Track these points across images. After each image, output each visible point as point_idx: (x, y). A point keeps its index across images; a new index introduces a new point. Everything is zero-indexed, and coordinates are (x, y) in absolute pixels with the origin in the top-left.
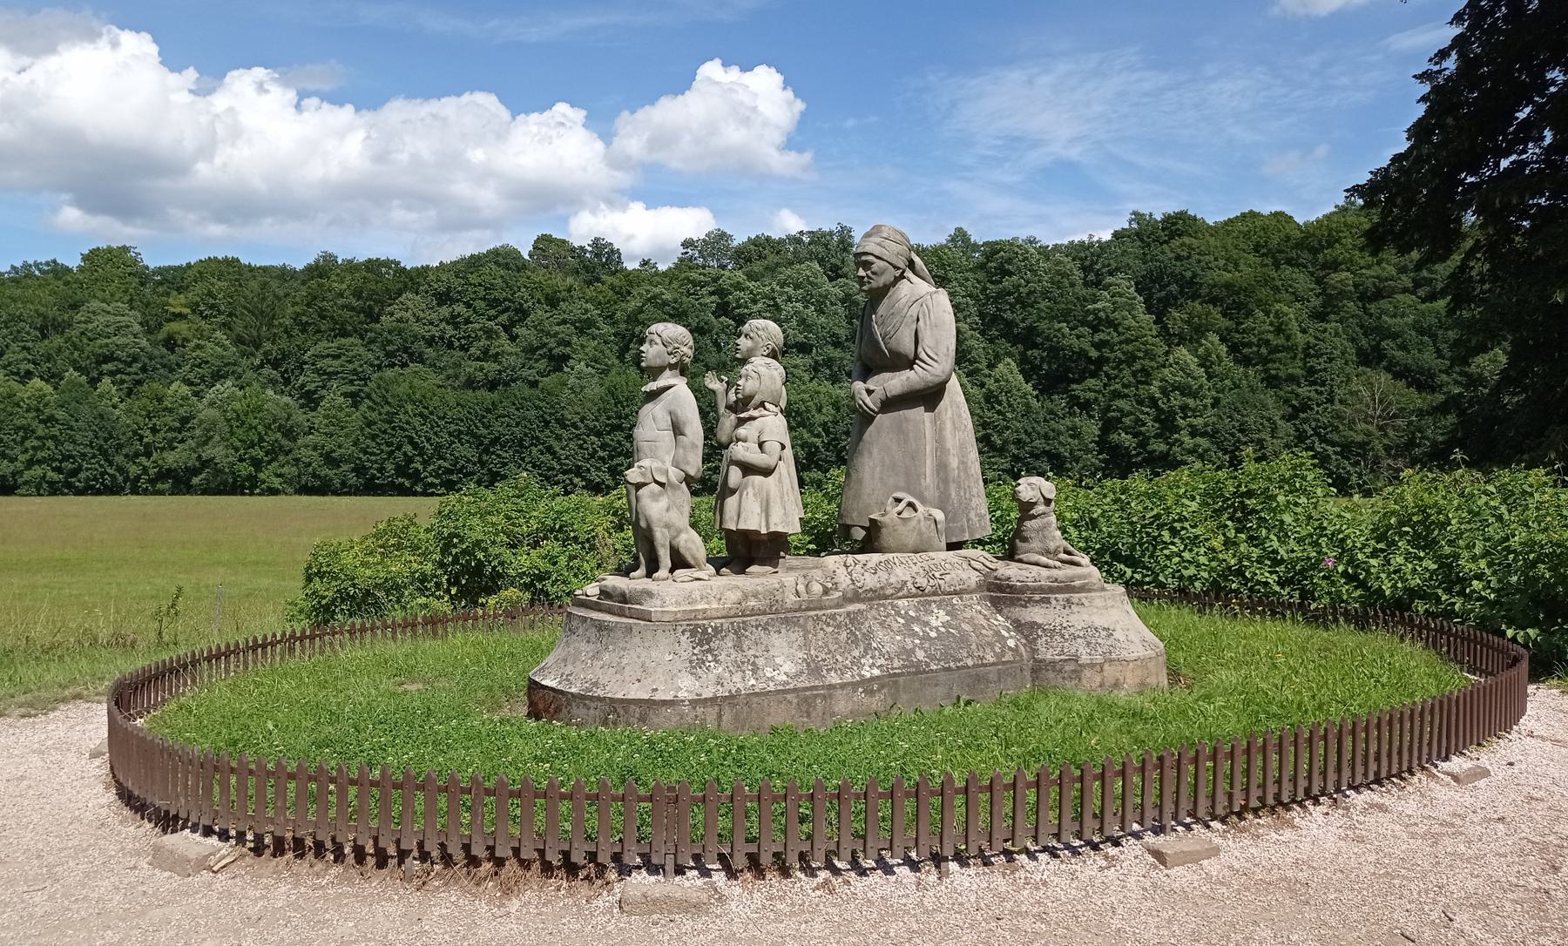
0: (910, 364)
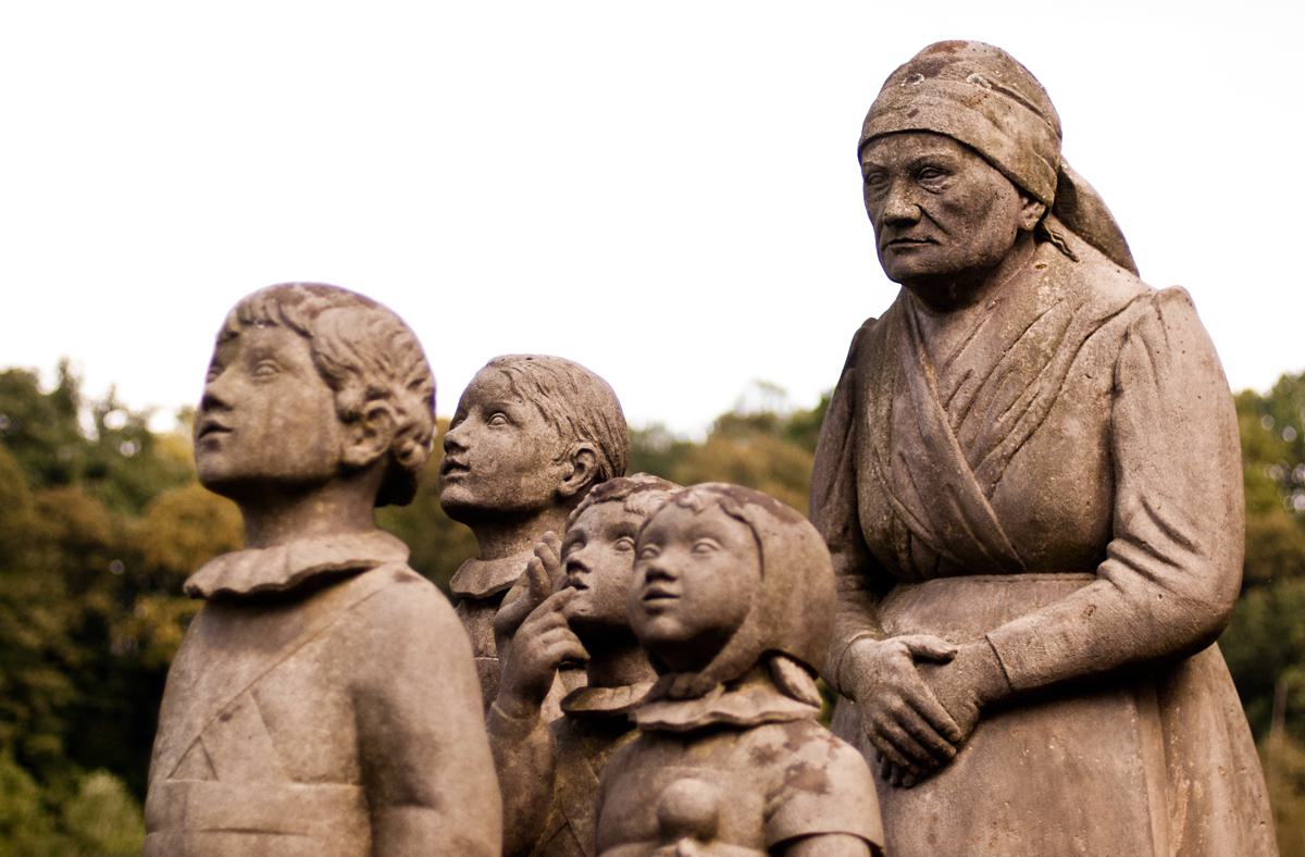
0: (1084, 556)
